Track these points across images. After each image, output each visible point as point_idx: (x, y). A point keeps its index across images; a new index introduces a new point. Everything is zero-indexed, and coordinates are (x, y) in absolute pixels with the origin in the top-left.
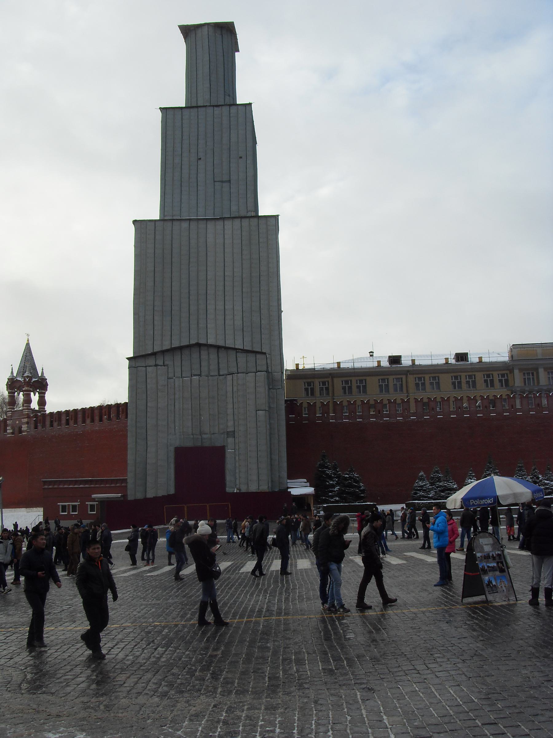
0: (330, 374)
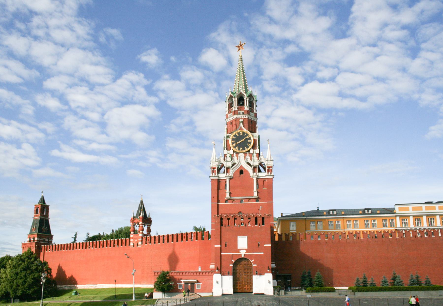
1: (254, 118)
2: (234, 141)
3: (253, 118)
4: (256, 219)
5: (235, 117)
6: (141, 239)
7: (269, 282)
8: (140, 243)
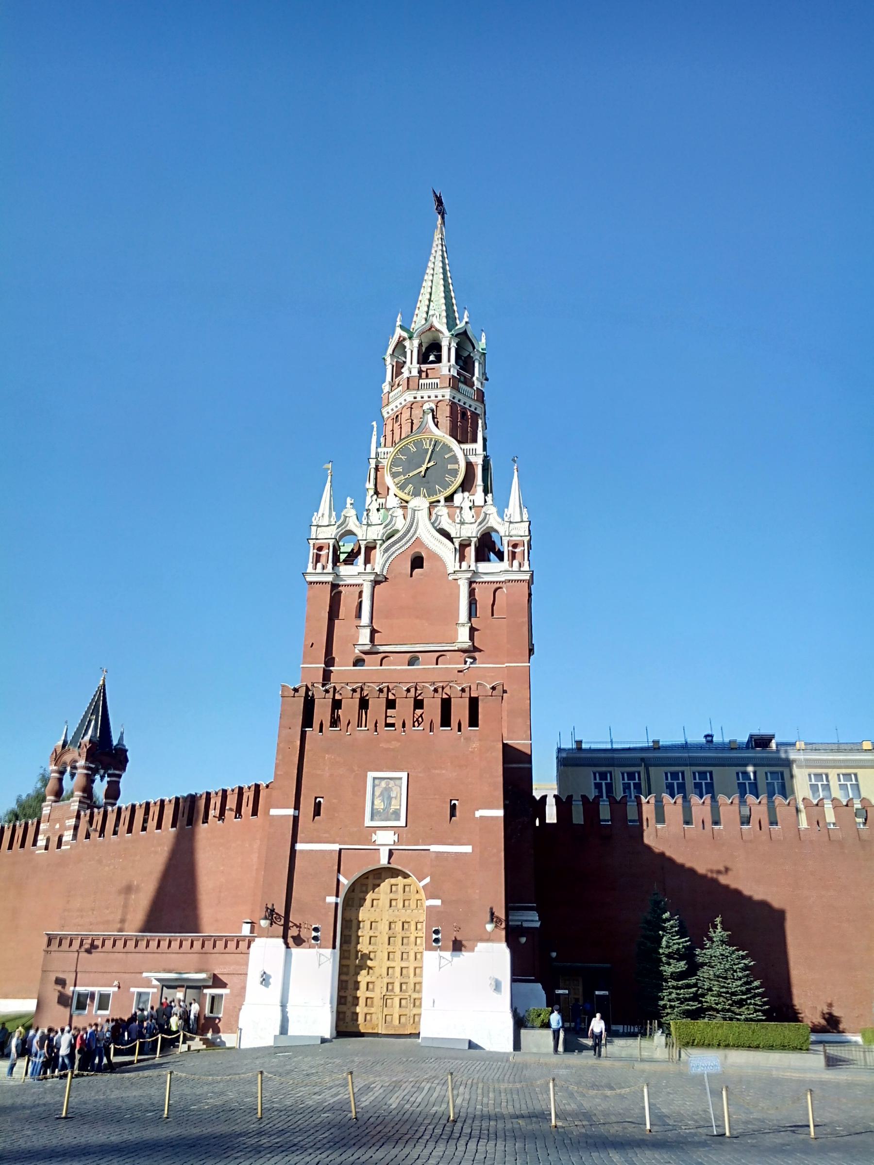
0: (642, 759)
2: (400, 469)
3: (469, 402)
4: (446, 704)
5: (409, 397)
6: (72, 822)
7: (497, 987)
8: (68, 836)
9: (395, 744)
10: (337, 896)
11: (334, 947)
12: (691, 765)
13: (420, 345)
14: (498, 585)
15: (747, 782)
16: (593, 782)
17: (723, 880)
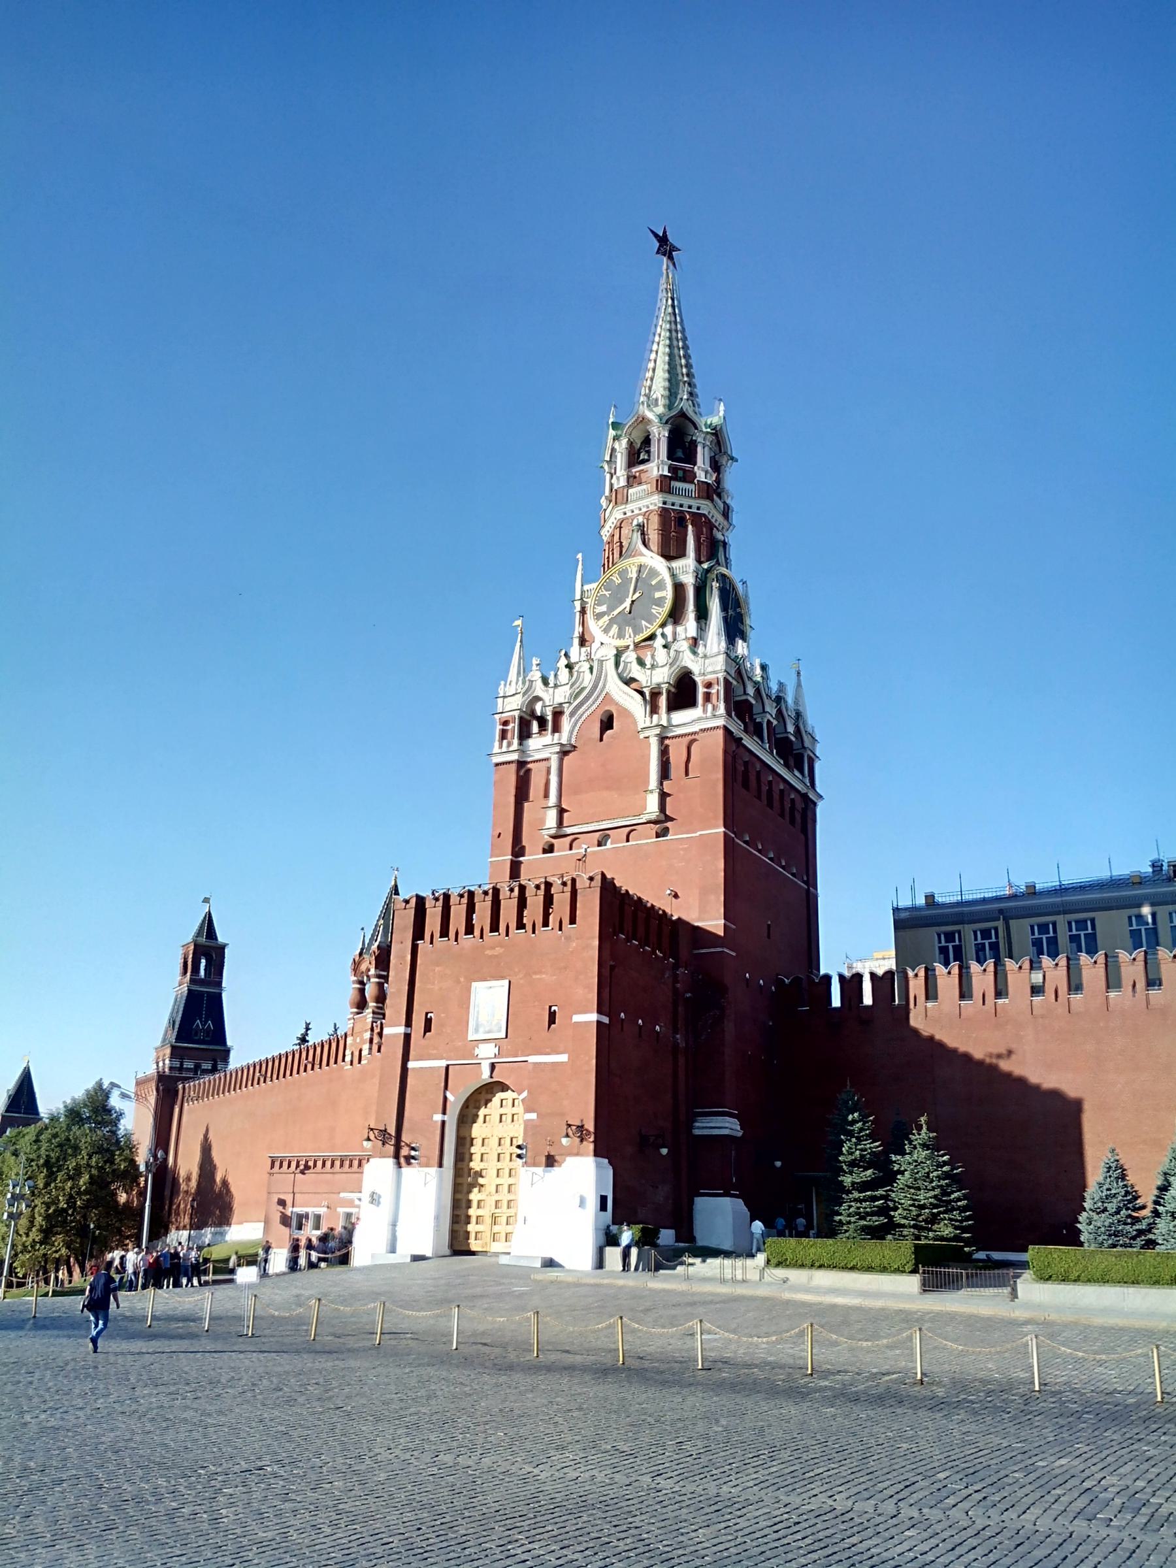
1: (694, 503)
3: (686, 502)
6: (367, 1035)
7: (582, 1203)
9: (498, 950)
10: (444, 1113)
11: (440, 1165)
12: (1065, 913)
13: (631, 444)
14: (690, 737)
15: (1143, 928)
16: (937, 945)
17: (1005, 1065)
